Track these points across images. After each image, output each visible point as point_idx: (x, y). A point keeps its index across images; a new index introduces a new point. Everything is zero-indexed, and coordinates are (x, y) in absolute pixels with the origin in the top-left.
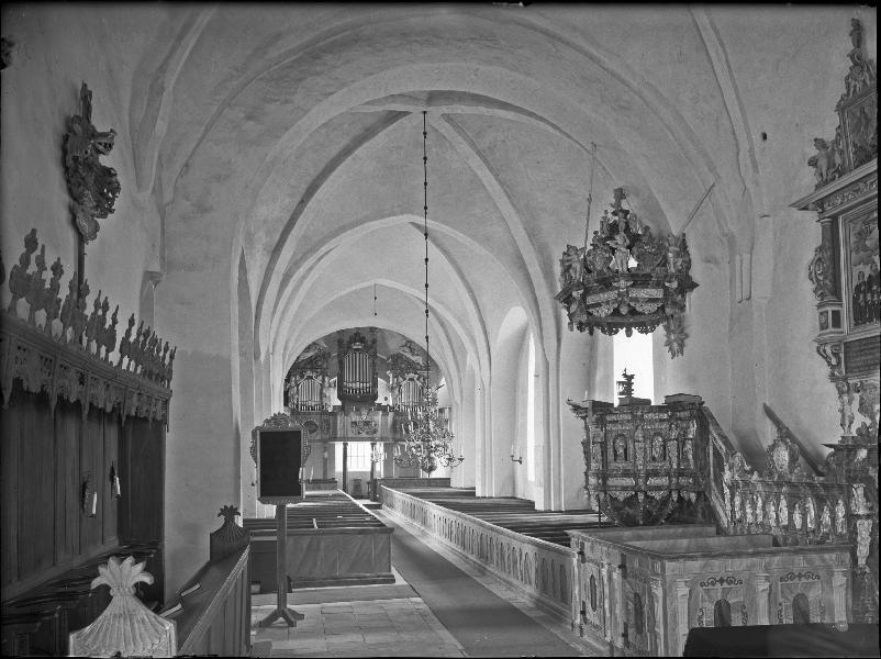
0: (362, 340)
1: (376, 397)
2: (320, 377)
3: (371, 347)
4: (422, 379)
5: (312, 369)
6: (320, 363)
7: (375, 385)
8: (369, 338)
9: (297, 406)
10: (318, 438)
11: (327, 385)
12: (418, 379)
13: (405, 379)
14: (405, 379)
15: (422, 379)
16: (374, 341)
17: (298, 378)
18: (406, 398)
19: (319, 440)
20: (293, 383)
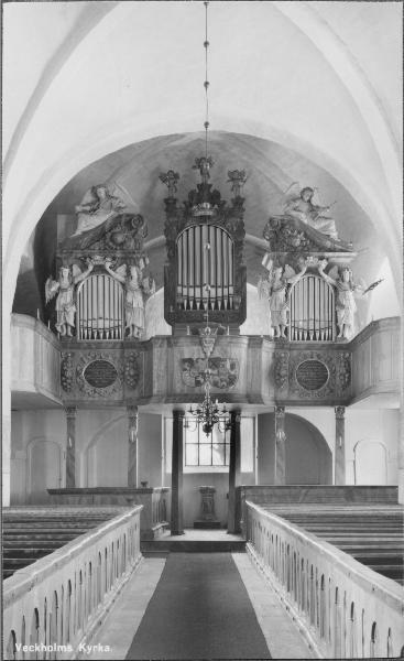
0: (215, 198)
1: (240, 317)
2: (122, 269)
3: (231, 213)
4: (334, 271)
5: (104, 252)
6: (120, 239)
7: (241, 292)
8: (227, 196)
9: (74, 330)
10: (117, 397)
11: (134, 283)
12: (327, 271)
13: (298, 270)
14: (298, 270)
15: (334, 271)
16: (239, 202)
17: (76, 269)
18: (304, 312)
19: (120, 404)
20: (65, 282)
